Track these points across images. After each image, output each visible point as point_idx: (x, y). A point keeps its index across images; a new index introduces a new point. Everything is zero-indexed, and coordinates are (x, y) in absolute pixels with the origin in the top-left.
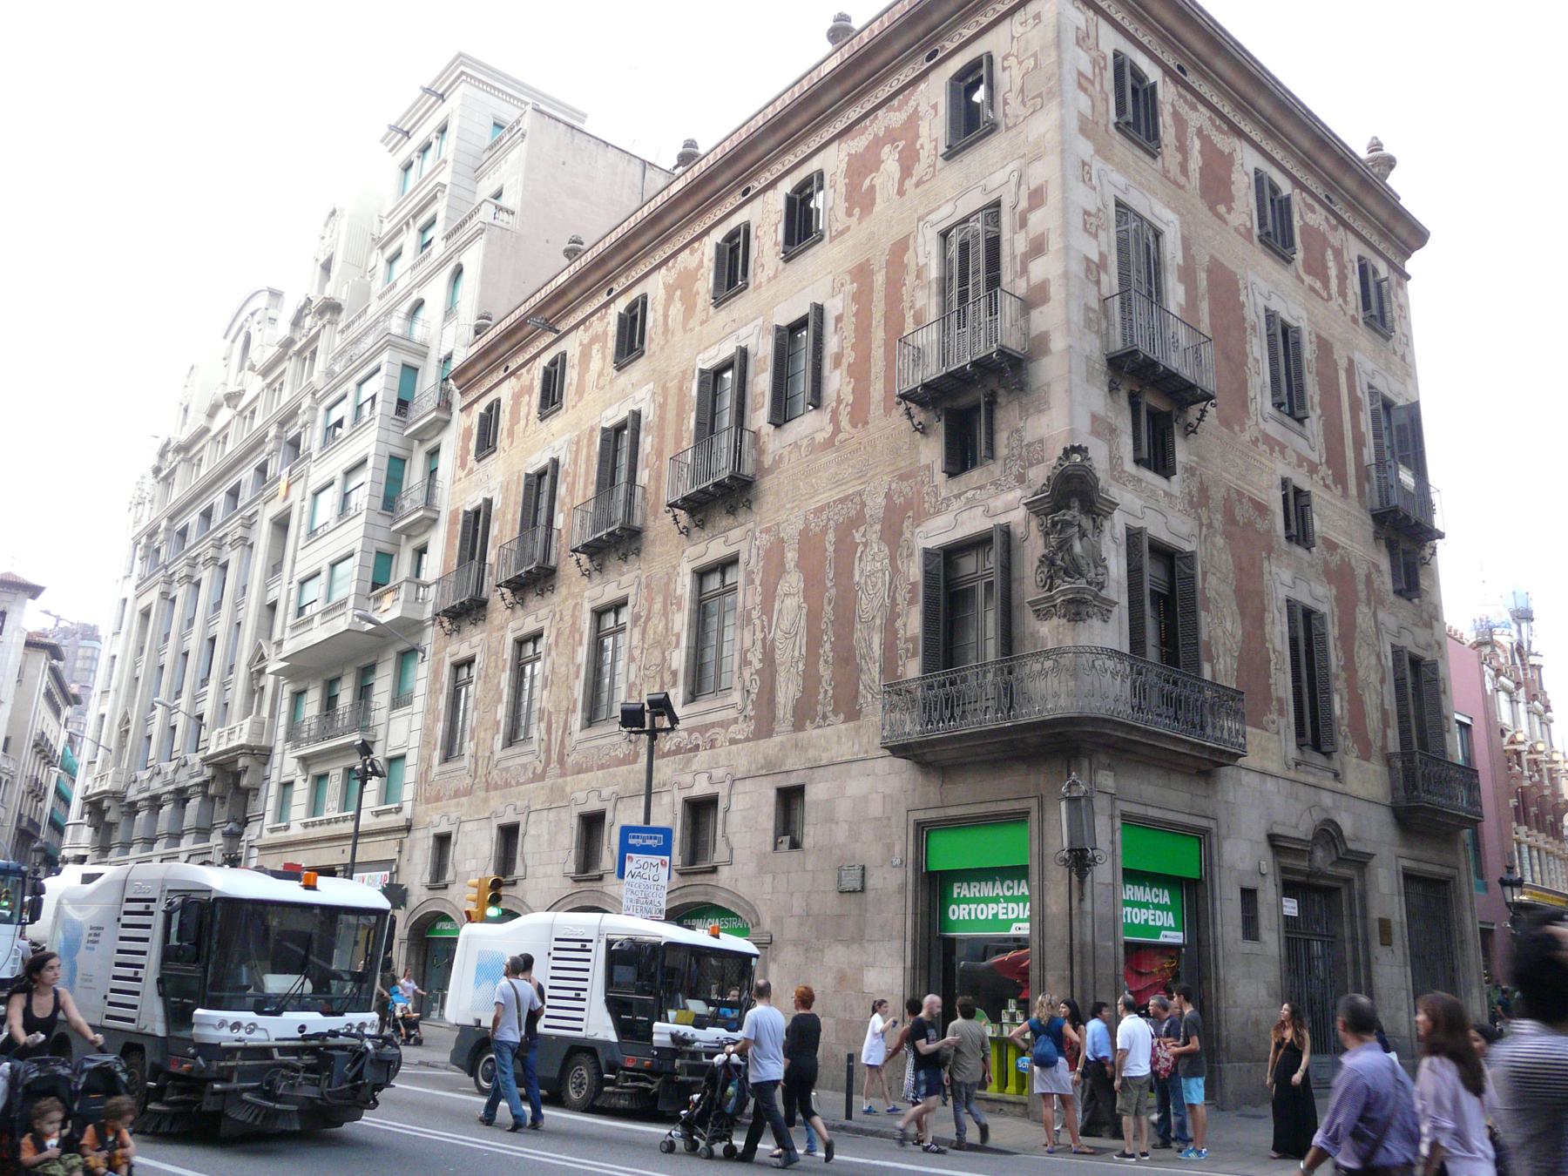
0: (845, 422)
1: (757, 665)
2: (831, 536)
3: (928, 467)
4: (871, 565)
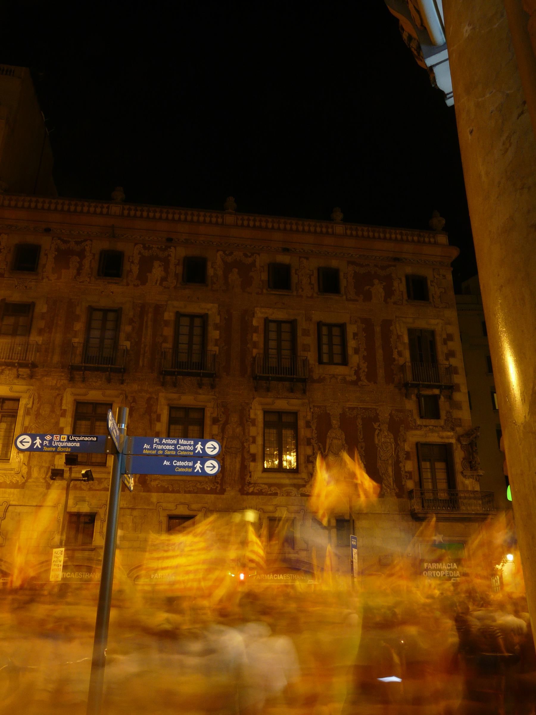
2: (359, 421)
3: (410, 411)
4: (383, 438)
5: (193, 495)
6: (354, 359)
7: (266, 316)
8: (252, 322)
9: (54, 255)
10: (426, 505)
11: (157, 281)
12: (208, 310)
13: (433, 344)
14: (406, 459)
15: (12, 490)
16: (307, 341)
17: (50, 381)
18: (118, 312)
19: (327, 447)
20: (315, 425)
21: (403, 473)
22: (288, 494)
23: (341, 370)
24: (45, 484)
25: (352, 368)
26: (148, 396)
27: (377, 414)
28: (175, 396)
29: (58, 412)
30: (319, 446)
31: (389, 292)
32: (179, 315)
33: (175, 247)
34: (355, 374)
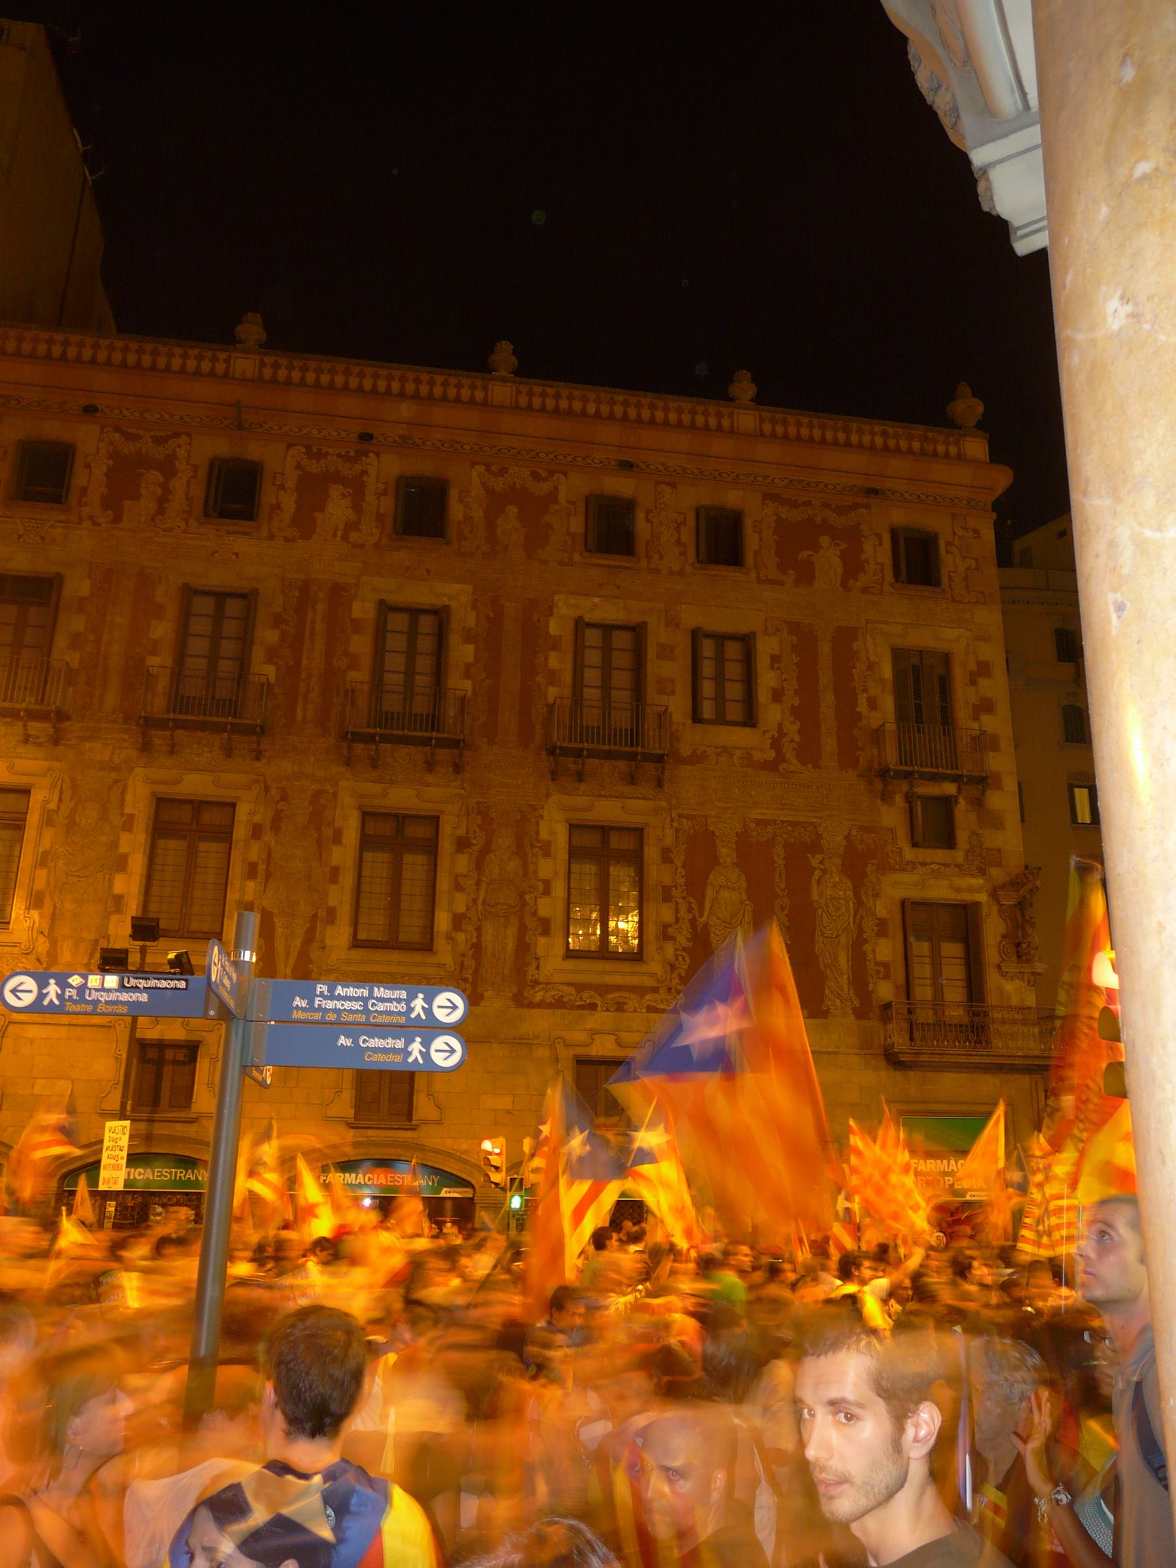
0: (790, 754)
1: (683, 940)
2: (779, 853)
3: (891, 830)
4: (830, 889)
6: (772, 714)
7: (579, 613)
8: (548, 627)
9: (105, 468)
10: (917, 1035)
11: (336, 529)
13: (945, 685)
16: (668, 670)
17: (98, 751)
18: (248, 597)
20: (682, 857)
21: (871, 966)
22: (620, 1007)
23: (740, 737)
25: (765, 732)
28: (377, 788)
29: (117, 820)
31: (853, 566)
32: (385, 608)
33: (378, 455)
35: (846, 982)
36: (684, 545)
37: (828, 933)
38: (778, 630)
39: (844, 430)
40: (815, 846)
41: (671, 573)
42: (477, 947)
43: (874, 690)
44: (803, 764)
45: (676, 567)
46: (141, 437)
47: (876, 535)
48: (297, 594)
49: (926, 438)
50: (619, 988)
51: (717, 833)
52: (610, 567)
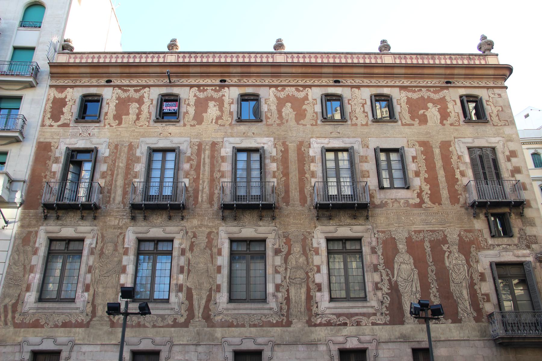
0: (427, 200)
1: (386, 289)
2: (427, 245)
3: (480, 230)
4: (454, 260)
5: (259, 328)
6: (417, 182)
7: (322, 145)
9: (115, 104)
11: (212, 120)
12: (264, 144)
13: (495, 162)
14: (480, 281)
15: (78, 329)
19: (396, 272)
21: (479, 296)
22: (358, 324)
23: (403, 194)
24: (109, 323)
25: (414, 191)
26: (208, 230)
27: (446, 236)
29: (121, 251)
30: (387, 272)
31: (444, 115)
34: (418, 196)
35: (468, 305)
36: (367, 113)
37: (456, 281)
38: (414, 145)
39: (432, 59)
40: (444, 241)
41: (362, 125)
42: (288, 299)
43: (462, 167)
44: (434, 204)
45: (364, 123)
46: (129, 90)
47: (453, 100)
48: (197, 148)
49: (470, 58)
50: (357, 314)
51: (397, 238)
52: (334, 125)
